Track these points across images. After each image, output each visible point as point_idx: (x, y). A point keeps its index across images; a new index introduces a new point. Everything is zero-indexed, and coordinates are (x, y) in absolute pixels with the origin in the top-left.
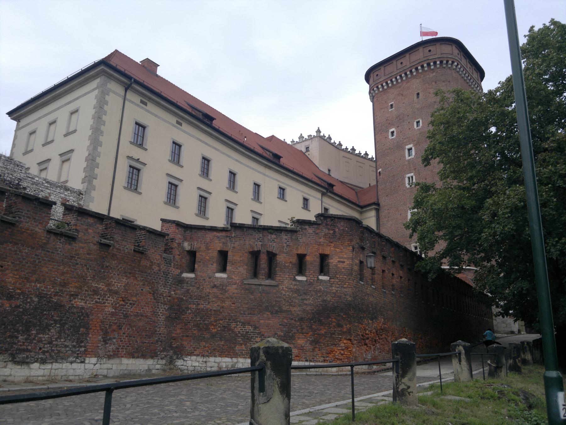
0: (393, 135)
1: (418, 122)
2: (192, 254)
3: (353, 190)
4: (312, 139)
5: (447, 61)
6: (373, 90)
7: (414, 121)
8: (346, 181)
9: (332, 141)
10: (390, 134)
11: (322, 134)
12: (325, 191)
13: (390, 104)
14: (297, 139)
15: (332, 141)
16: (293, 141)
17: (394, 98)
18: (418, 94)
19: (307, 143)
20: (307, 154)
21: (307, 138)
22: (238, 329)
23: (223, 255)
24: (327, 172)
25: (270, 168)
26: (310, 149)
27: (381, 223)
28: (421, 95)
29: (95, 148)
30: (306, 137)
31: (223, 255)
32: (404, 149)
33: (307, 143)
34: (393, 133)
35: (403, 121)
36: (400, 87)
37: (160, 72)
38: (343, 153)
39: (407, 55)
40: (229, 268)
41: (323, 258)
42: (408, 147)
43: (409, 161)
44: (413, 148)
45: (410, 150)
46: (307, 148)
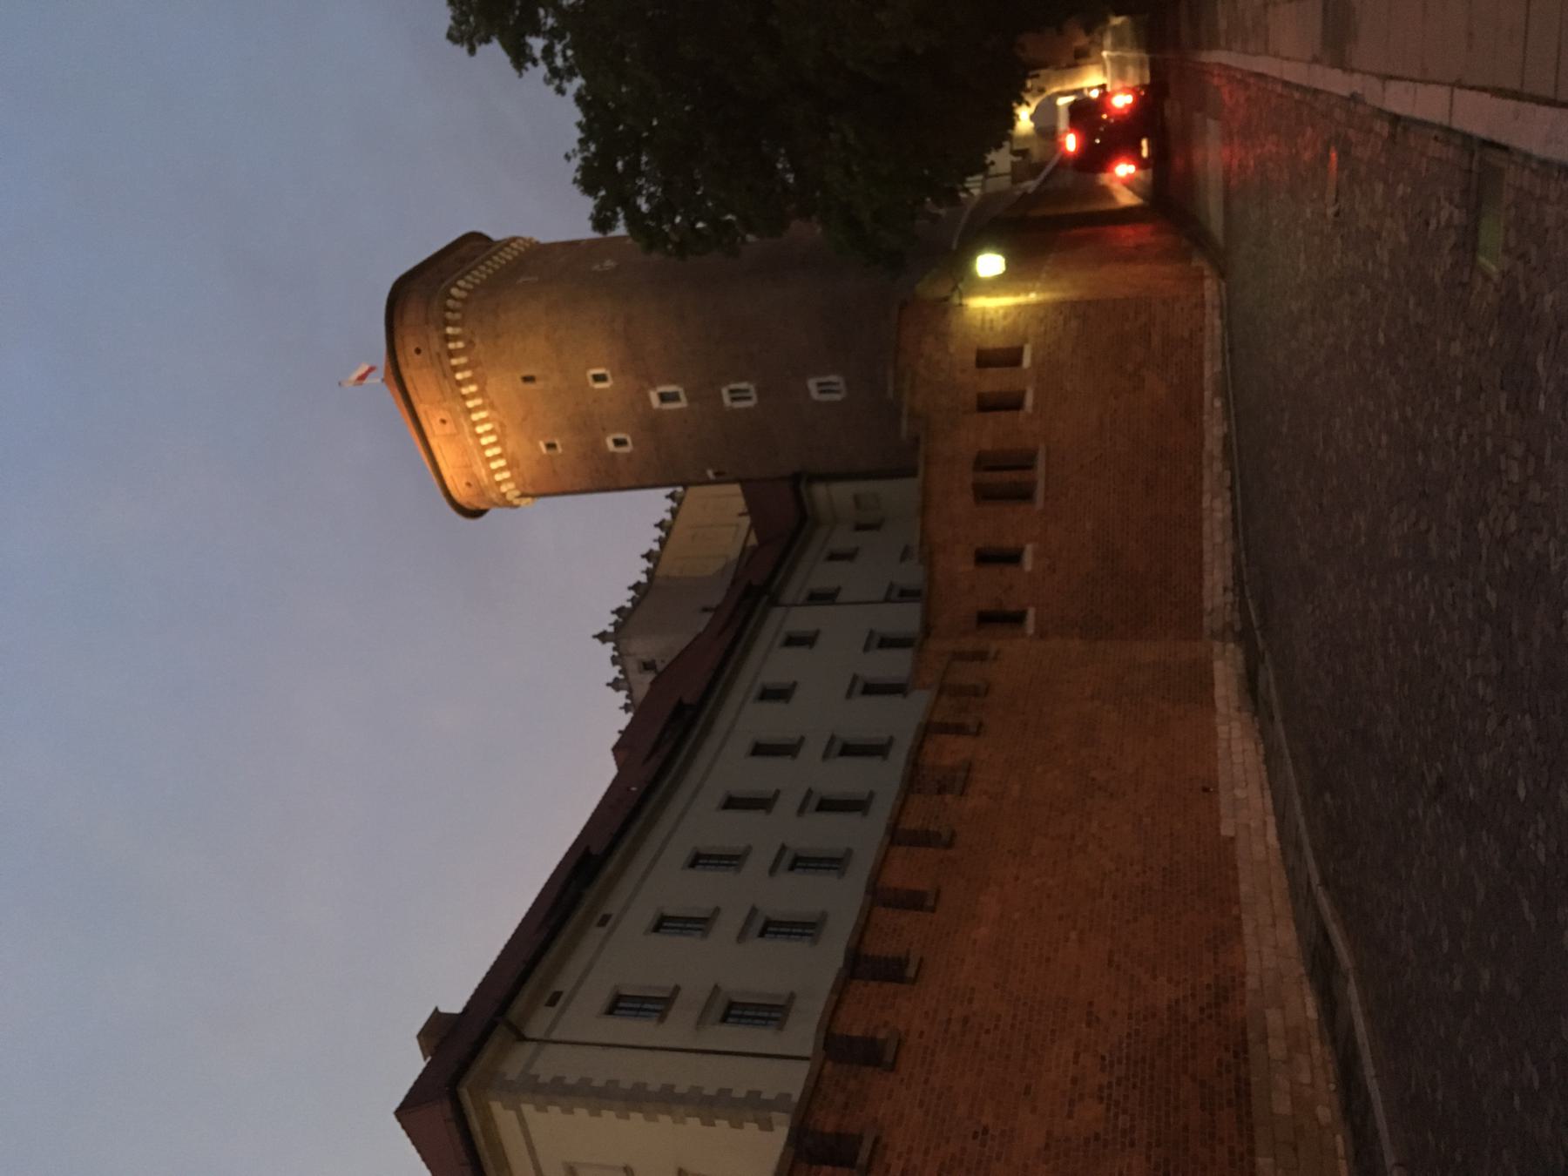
1: (598, 378)
4: (621, 655)
7: (593, 389)
9: (629, 605)
11: (611, 629)
12: (765, 598)
14: (621, 697)
15: (629, 605)
16: (626, 708)
20: (660, 667)
21: (618, 668)
23: (984, 558)
24: (709, 616)
25: (710, 723)
26: (645, 658)
28: (528, 373)
29: (682, 1099)
30: (615, 672)
31: (984, 558)
32: (660, 412)
33: (632, 665)
34: (618, 443)
37: (455, 1004)
40: (1009, 542)
43: (690, 400)
45: (664, 397)
46: (647, 666)
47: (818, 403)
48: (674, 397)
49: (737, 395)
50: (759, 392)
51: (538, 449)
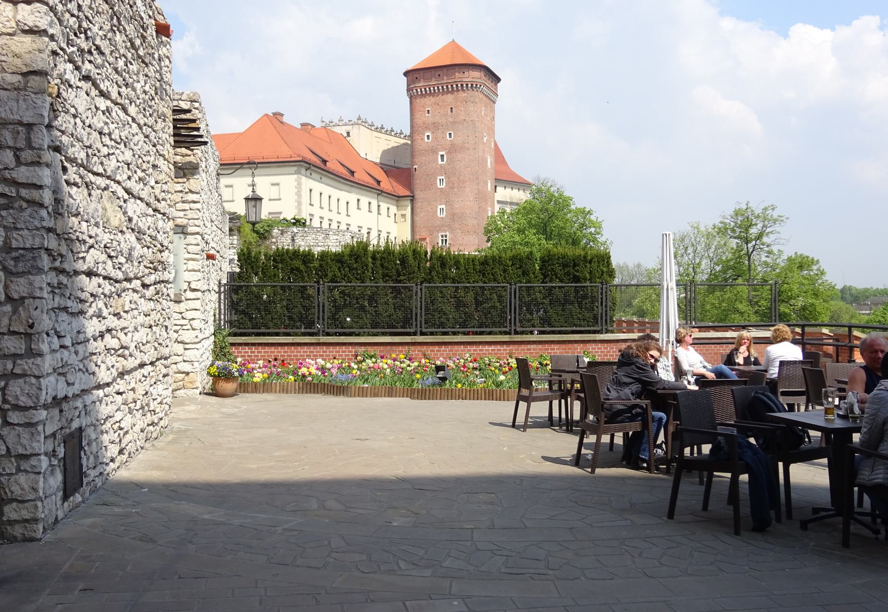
1: (450, 134)
5: (476, 85)
6: (412, 90)
13: (427, 109)
17: (431, 105)
18: (451, 108)
19: (348, 128)
27: (415, 212)
34: (428, 136)
35: (438, 129)
37: (285, 119)
39: (445, 70)
42: (441, 153)
44: (445, 156)
45: (442, 156)
47: (437, 207)
48: (443, 160)
50: (442, 189)
51: (428, 107)
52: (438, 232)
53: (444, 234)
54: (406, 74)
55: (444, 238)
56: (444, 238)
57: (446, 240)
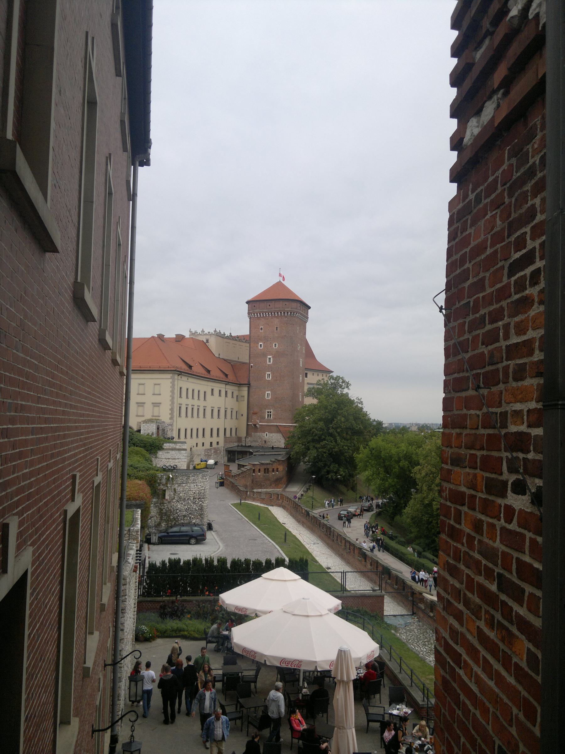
0: (261, 347)
1: (275, 345)
2: (254, 470)
3: (230, 363)
8: (226, 358)
10: (259, 345)
20: (207, 344)
22: (262, 484)
23: (259, 470)
26: (209, 341)
28: (278, 329)
31: (259, 470)
32: (267, 357)
33: (208, 337)
36: (267, 319)
38: (226, 340)
39: (273, 302)
41: (277, 469)
46: (207, 341)
47: (265, 392)
49: (269, 375)
50: (269, 380)
52: (265, 409)
53: (269, 411)
54: (248, 302)
55: (269, 414)
56: (269, 414)
57: (270, 415)
